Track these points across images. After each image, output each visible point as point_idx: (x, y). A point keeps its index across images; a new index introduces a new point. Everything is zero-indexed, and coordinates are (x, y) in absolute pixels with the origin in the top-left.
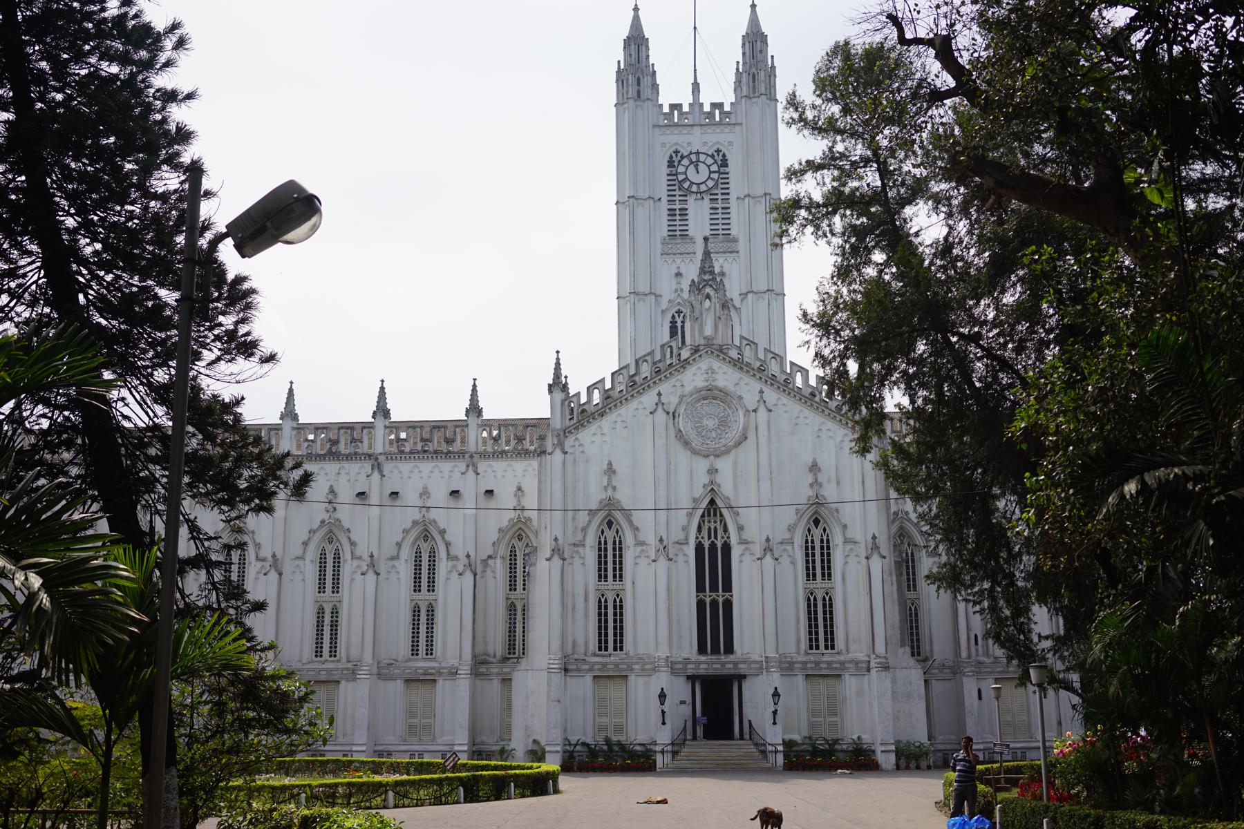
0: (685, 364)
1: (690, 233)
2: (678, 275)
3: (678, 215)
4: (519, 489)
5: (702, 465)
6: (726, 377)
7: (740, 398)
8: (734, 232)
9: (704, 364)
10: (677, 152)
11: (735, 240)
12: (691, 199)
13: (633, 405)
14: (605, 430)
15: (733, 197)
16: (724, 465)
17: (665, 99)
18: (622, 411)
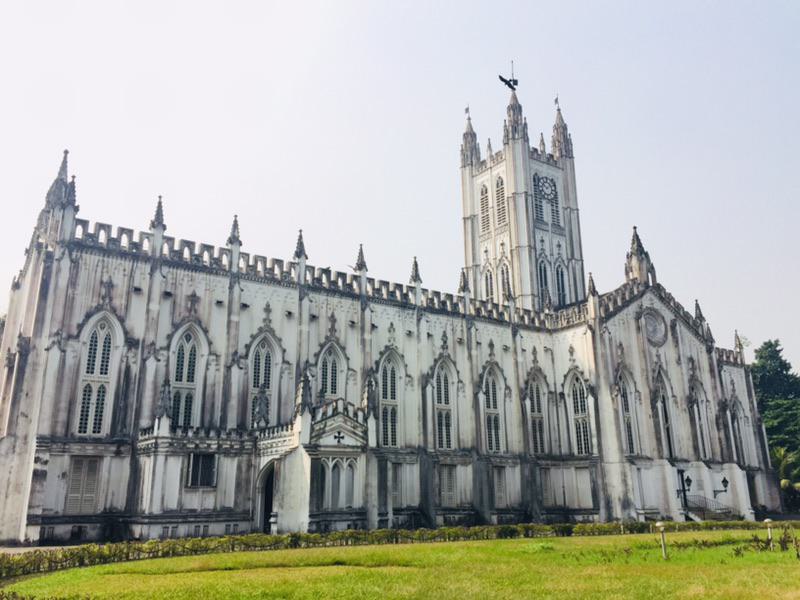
0: (642, 294)
1: (545, 219)
2: (542, 241)
3: (539, 208)
4: (535, 349)
5: (654, 351)
6: (658, 305)
7: (663, 318)
8: (562, 224)
9: (648, 296)
10: (536, 174)
11: (563, 229)
12: (544, 202)
13: (625, 311)
14: (617, 323)
15: (560, 206)
16: (662, 351)
17: (534, 143)
18: (621, 314)
